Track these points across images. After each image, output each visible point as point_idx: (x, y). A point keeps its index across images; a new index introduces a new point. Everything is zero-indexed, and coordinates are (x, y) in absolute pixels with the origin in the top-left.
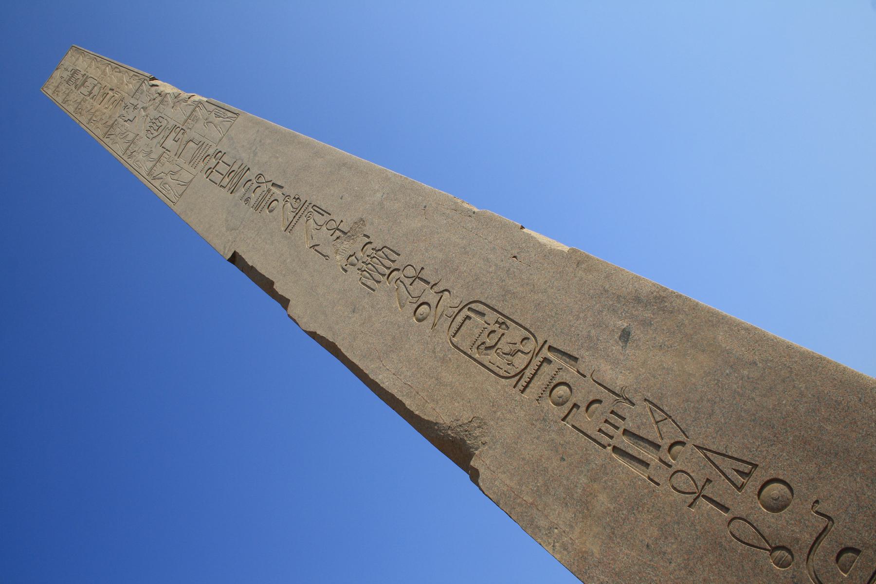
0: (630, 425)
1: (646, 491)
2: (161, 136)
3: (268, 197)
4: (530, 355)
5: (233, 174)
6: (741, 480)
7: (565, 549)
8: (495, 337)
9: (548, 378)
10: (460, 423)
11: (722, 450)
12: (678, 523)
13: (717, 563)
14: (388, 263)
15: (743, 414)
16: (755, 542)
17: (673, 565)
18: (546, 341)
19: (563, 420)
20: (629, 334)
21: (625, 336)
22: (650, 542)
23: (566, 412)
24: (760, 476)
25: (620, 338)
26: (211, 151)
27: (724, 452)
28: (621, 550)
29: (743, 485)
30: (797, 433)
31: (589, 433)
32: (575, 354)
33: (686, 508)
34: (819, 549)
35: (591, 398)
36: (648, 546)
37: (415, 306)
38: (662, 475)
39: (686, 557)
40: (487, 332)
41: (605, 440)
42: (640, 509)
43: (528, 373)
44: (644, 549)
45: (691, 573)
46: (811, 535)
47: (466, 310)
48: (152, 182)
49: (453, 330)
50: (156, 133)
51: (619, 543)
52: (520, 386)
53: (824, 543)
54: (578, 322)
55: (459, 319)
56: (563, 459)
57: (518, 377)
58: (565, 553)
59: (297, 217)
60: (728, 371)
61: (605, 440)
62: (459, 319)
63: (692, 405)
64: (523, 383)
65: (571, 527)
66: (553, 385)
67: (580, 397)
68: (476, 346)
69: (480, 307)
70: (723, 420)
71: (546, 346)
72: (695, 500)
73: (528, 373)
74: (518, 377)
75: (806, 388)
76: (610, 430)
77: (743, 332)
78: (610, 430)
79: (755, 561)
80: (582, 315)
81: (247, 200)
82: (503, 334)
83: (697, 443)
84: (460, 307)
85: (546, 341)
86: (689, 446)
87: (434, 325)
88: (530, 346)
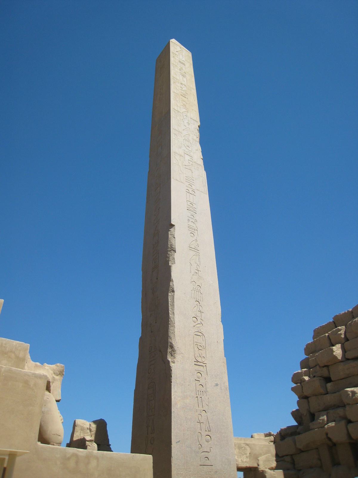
0: (203, 398)
2: (187, 151)
3: (194, 231)
5: (192, 205)
6: (207, 430)
8: (200, 348)
14: (199, 299)
19: (195, 380)
21: (217, 385)
26: (193, 187)
29: (206, 431)
31: (197, 388)
35: (202, 384)
37: (195, 317)
38: (198, 413)
41: (197, 394)
43: (199, 363)
45: (187, 430)
47: (202, 334)
48: (174, 158)
49: (196, 333)
50: (186, 145)
53: (206, 453)
55: (199, 334)
59: (194, 250)
61: (197, 394)
62: (199, 334)
64: (196, 363)
67: (202, 381)
69: (204, 339)
71: (206, 365)
73: (199, 363)
76: (200, 394)
78: (200, 394)
81: (189, 220)
86: (206, 415)
87: (194, 326)
88: (203, 360)
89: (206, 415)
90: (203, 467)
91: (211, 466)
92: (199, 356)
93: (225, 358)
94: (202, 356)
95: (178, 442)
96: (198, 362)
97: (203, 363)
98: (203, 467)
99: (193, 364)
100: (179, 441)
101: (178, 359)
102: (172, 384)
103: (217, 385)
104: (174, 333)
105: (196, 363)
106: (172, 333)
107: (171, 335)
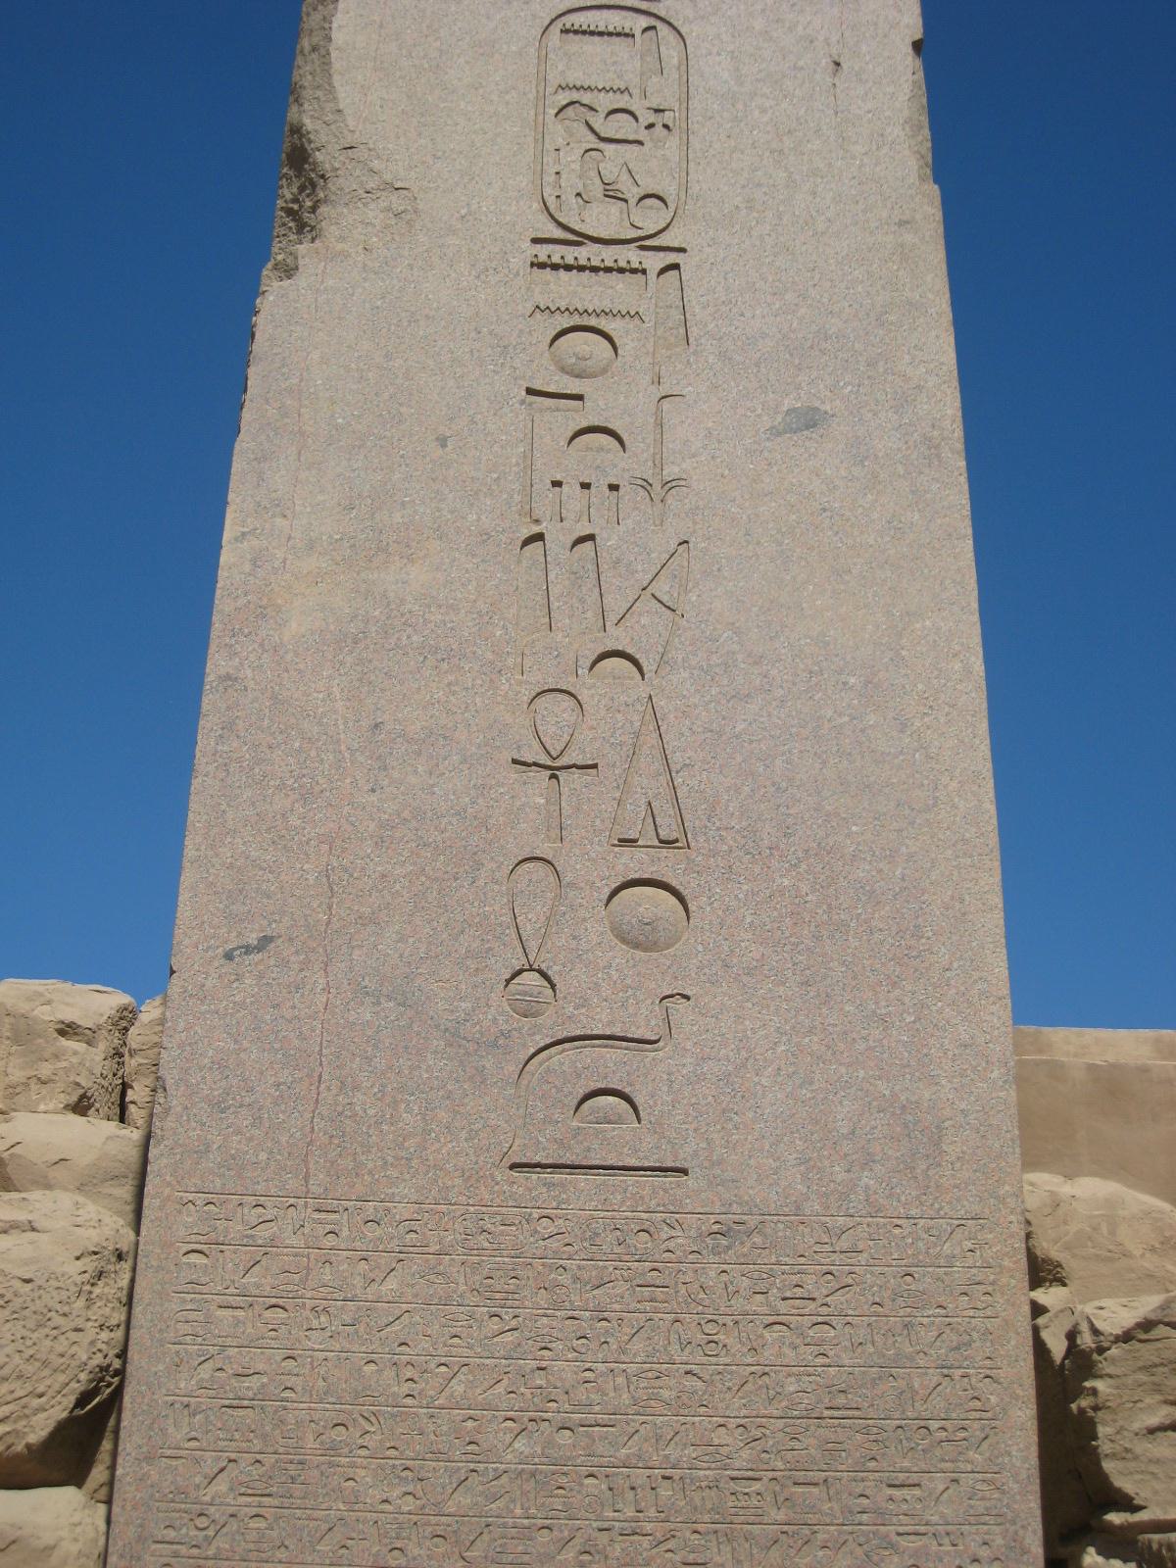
1: (490, 656)
4: (632, 234)
7: (254, 562)
8: (621, 127)
9: (606, 305)
10: (376, 164)
11: (677, 759)
12: (464, 761)
13: (436, 879)
15: (778, 762)
16: (527, 930)
17: (374, 798)
18: (682, 250)
20: (811, 425)
22: (388, 727)
23: (551, 389)
24: (665, 865)
25: (788, 412)
27: (674, 768)
28: (330, 677)
30: (804, 888)
32: (694, 332)
33: (508, 756)
34: (589, 1053)
36: (376, 726)
39: (406, 814)
40: (622, 102)
42: (445, 666)
44: (365, 723)
46: (611, 1023)
47: (644, 22)
51: (342, 663)
52: (543, 252)
53: (612, 1054)
56: (443, 442)
57: (559, 234)
58: (247, 567)
60: (852, 680)
63: (736, 647)
64: (557, 253)
65: (311, 546)
66: (593, 322)
68: (575, 96)
69: (672, 53)
70: (740, 727)
72: (535, 764)
74: (559, 234)
75: (911, 856)
77: (958, 666)
79: (490, 949)
82: (640, 143)
83: (660, 703)
85: (682, 250)
86: (643, 690)
88: (650, 219)
89: (643, 690)
90: (550, 1185)
91: (670, 1180)
92: (598, 190)
93: (936, 187)
94: (633, 193)
95: (248, 950)
96: (582, 239)
97: (647, 243)
98: (550, 1185)
99: (519, 262)
100: (265, 941)
102: (244, 445)
103: (809, 420)
104: (321, 51)
105: (557, 253)
106: (314, 49)
107: (305, 73)
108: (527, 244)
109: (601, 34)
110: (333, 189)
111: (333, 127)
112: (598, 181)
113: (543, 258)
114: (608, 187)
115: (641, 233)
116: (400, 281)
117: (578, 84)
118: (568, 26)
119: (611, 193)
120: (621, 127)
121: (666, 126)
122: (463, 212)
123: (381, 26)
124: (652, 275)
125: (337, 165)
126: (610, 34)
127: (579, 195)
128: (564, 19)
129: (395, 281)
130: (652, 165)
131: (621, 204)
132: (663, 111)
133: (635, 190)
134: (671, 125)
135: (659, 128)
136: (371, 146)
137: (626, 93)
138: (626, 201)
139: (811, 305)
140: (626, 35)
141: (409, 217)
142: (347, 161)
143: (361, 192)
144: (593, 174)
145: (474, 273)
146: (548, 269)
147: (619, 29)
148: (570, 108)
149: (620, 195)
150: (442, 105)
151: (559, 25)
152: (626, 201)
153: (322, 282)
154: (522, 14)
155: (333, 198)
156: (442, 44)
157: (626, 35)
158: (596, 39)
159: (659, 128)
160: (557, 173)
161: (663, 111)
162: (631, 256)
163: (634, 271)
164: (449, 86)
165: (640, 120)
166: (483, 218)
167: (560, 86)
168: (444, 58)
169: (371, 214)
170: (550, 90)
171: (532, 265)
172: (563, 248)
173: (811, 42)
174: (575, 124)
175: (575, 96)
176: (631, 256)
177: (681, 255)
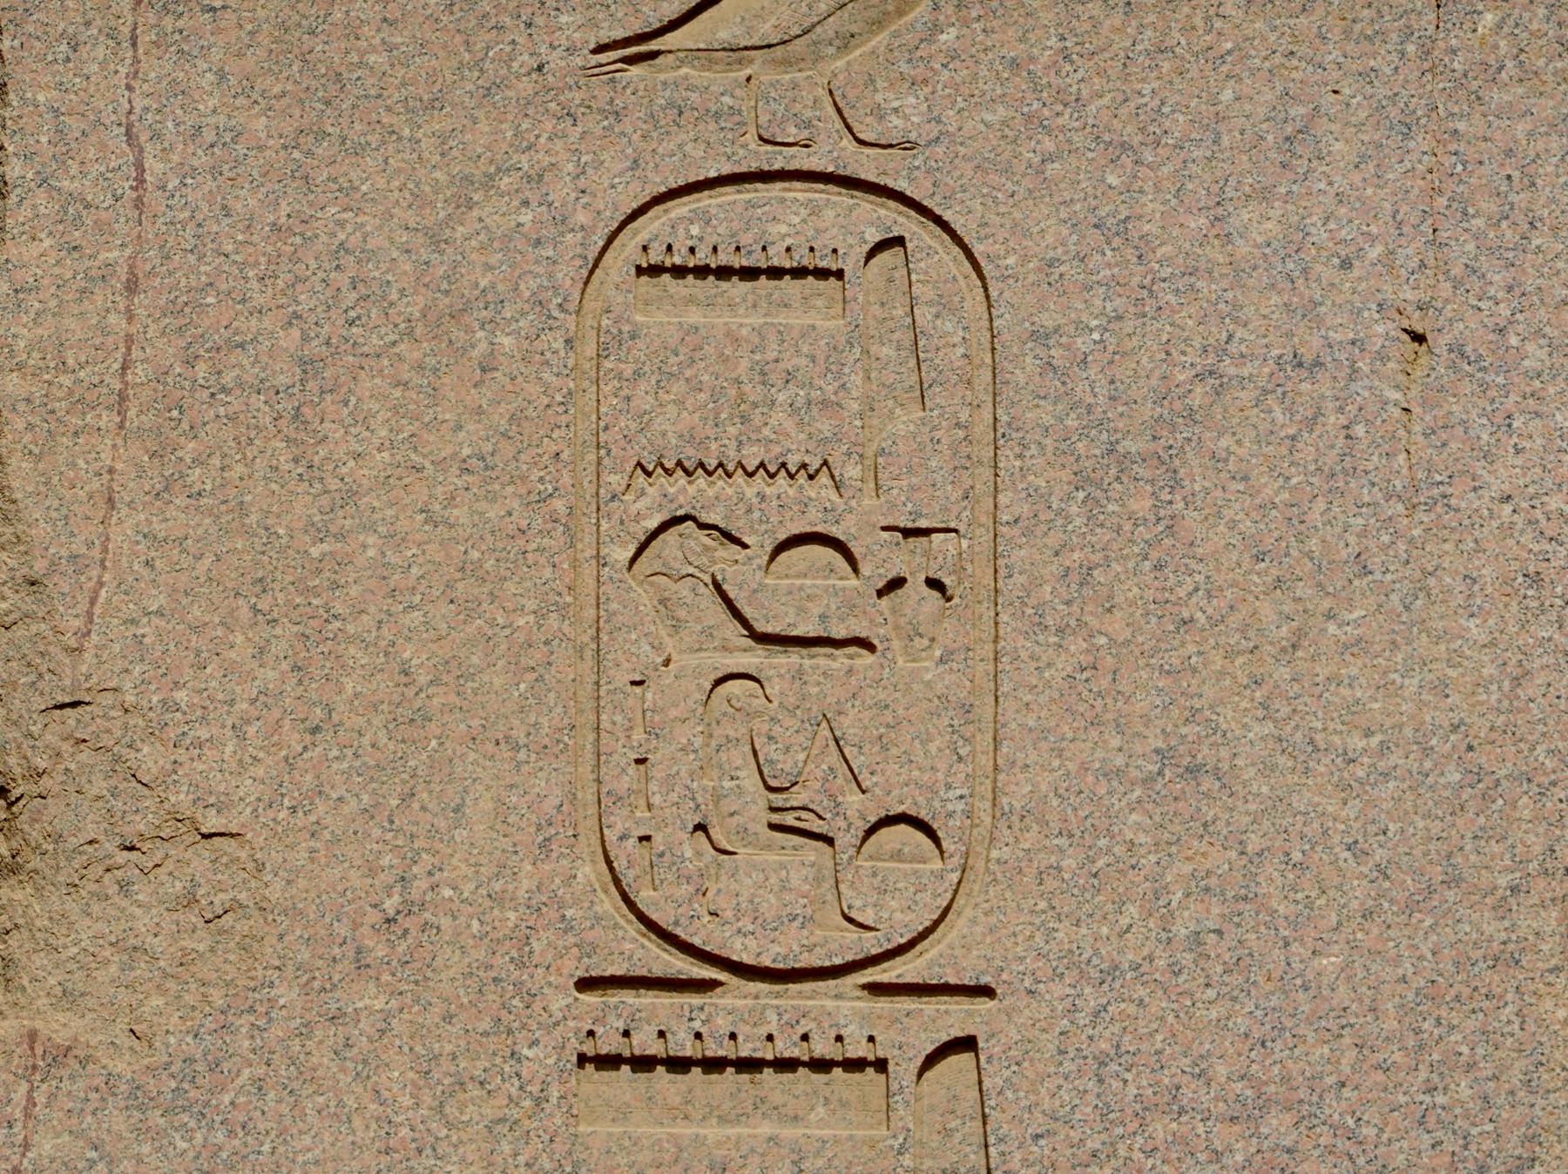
4: (847, 945)
8: (804, 593)
10: (150, 759)
49: (681, 228)
54: (1222, 1135)
55: (789, 221)
62: (789, 221)
64: (657, 1020)
68: (686, 493)
69: (953, 336)
80: (1277, 1124)
84: (867, 166)
99: (544, 1057)
101: (67, 997)
105: (657, 1020)
108: (561, 1000)
109: (749, 274)
110: (35, 835)
111: (19, 632)
112: (750, 781)
113: (609, 1044)
114: (778, 800)
115: (872, 944)
116: (231, 1134)
117: (691, 456)
118: (656, 256)
119: (789, 819)
120: (804, 593)
121: (934, 584)
122: (391, 905)
123: (132, 287)
124: (904, 1069)
125: (41, 764)
126: (776, 273)
127: (701, 827)
128: (651, 226)
129: (220, 1136)
130: (899, 715)
131: (813, 851)
132: (926, 532)
133: (853, 799)
134: (947, 581)
135: (916, 587)
136: (130, 699)
137: (823, 478)
138: (830, 841)
139: (1331, 1150)
140: (822, 274)
141: (243, 927)
142: (66, 747)
143: (110, 846)
144: (739, 757)
145: (427, 1099)
146: (625, 1068)
147: (802, 258)
148: (671, 536)
149: (816, 826)
150: (315, 552)
151: (628, 249)
152: (830, 841)
153: (26, 1146)
154: (526, 217)
155: (36, 862)
156: (305, 338)
157: (822, 274)
158: (737, 288)
159: (916, 587)
160: (640, 761)
161: (926, 532)
162: (842, 1015)
163: (855, 1065)
164: (334, 484)
165: (865, 569)
166: (445, 922)
167: (639, 464)
168: (310, 385)
169: (143, 922)
170: (615, 480)
171: (582, 1060)
172: (670, 1006)
173: (1346, 264)
174: (684, 589)
175: (686, 493)
176: (842, 1015)
177: (983, 1005)
